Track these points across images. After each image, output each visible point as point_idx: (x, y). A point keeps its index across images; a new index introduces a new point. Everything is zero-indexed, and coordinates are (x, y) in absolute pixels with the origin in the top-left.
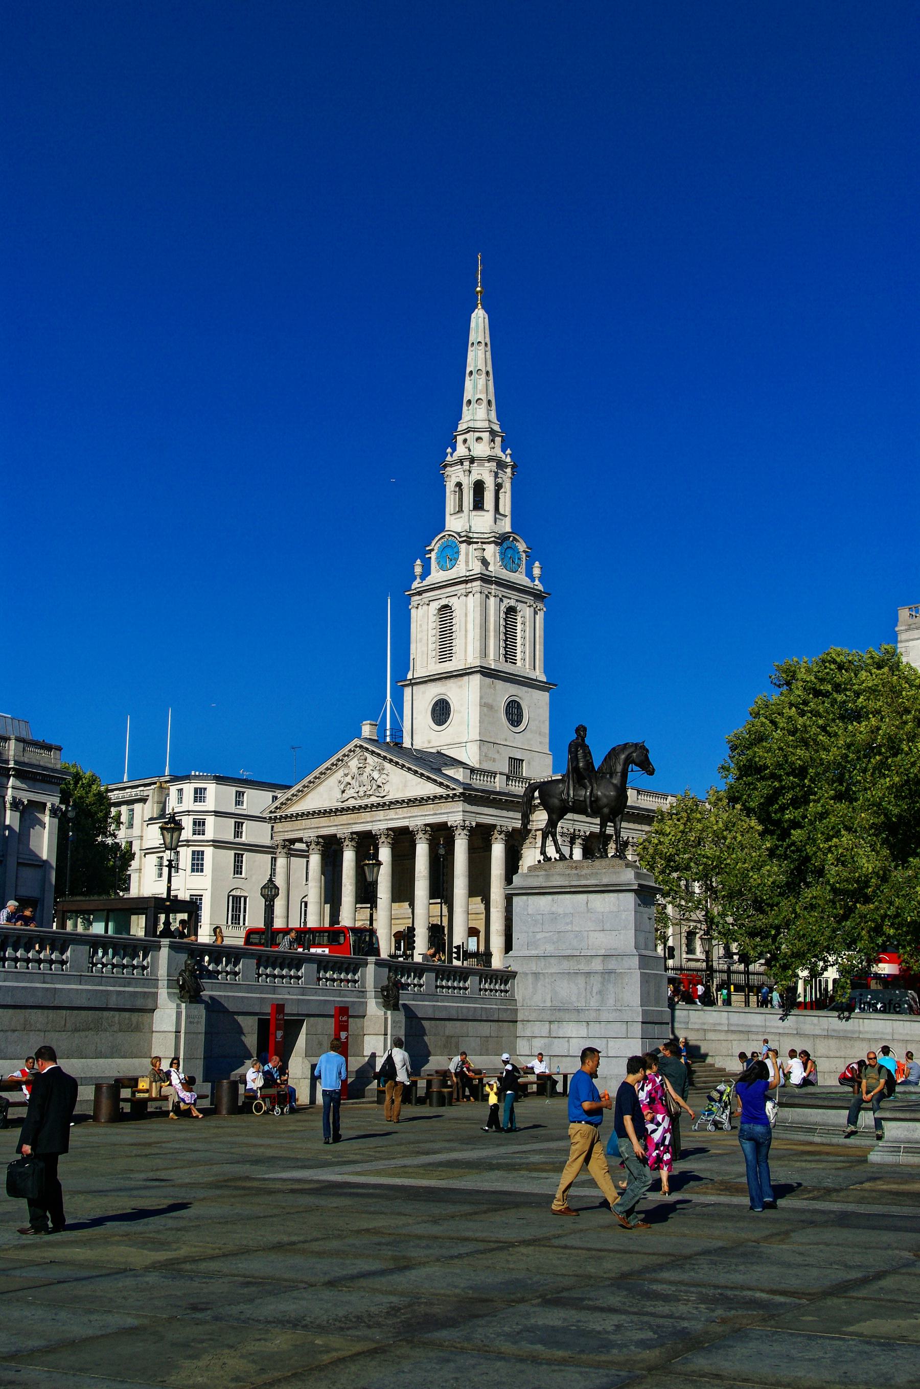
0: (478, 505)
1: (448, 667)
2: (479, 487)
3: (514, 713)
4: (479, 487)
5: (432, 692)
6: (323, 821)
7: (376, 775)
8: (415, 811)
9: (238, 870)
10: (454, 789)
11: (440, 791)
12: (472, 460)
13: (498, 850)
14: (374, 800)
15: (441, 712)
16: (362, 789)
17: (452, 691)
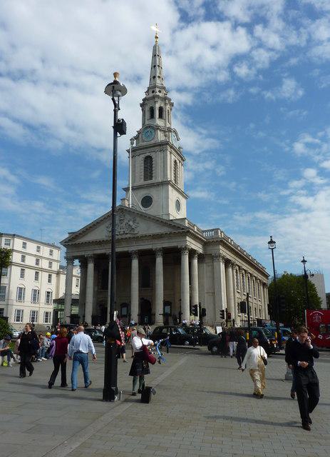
0: (161, 116)
1: (150, 182)
2: (161, 110)
3: (178, 204)
4: (161, 110)
5: (143, 193)
6: (97, 247)
7: (131, 223)
8: (156, 241)
9: (22, 276)
10: (183, 229)
11: (173, 231)
12: (158, 97)
13: (195, 261)
14: (131, 236)
15: (147, 201)
16: (122, 230)
17: (153, 193)
